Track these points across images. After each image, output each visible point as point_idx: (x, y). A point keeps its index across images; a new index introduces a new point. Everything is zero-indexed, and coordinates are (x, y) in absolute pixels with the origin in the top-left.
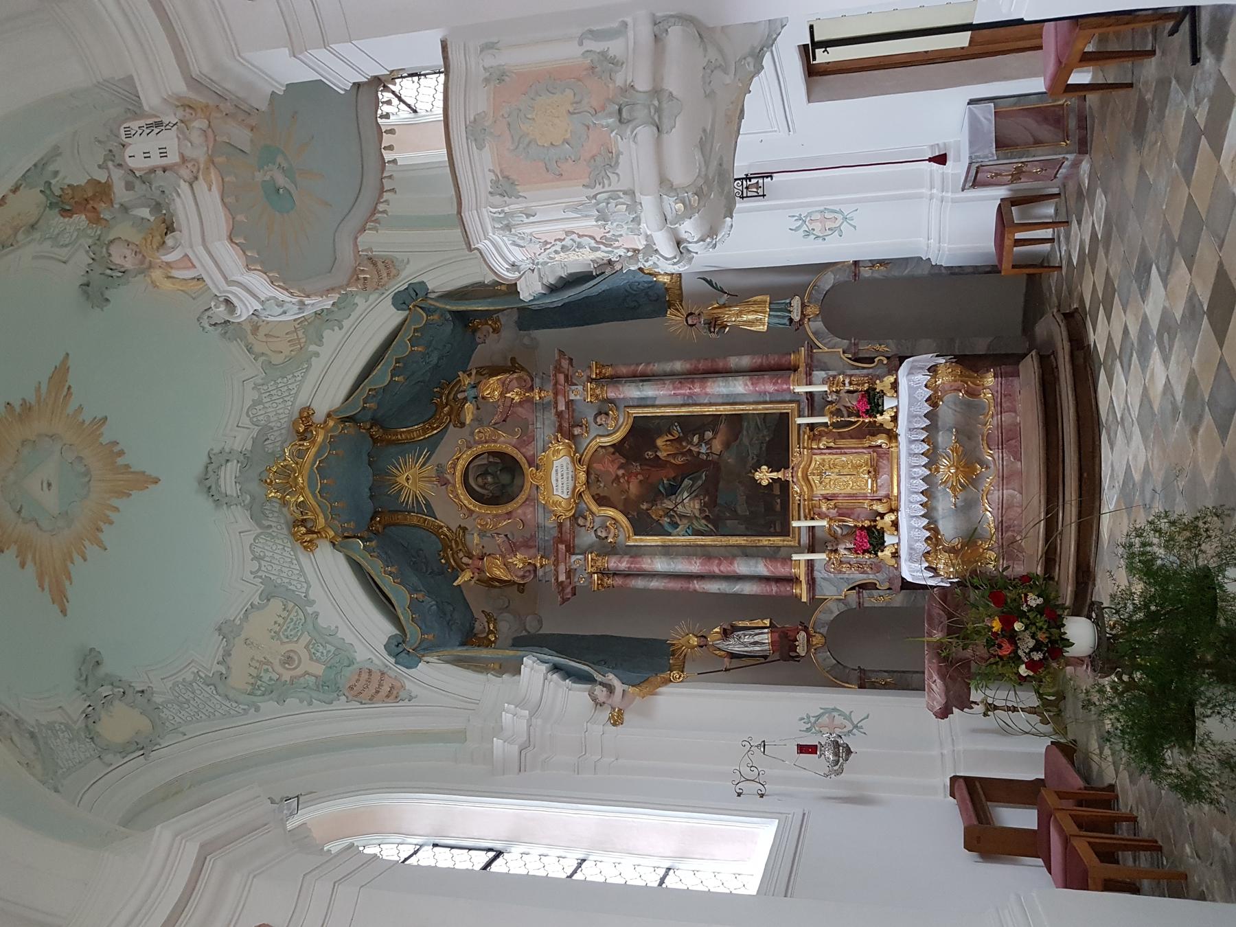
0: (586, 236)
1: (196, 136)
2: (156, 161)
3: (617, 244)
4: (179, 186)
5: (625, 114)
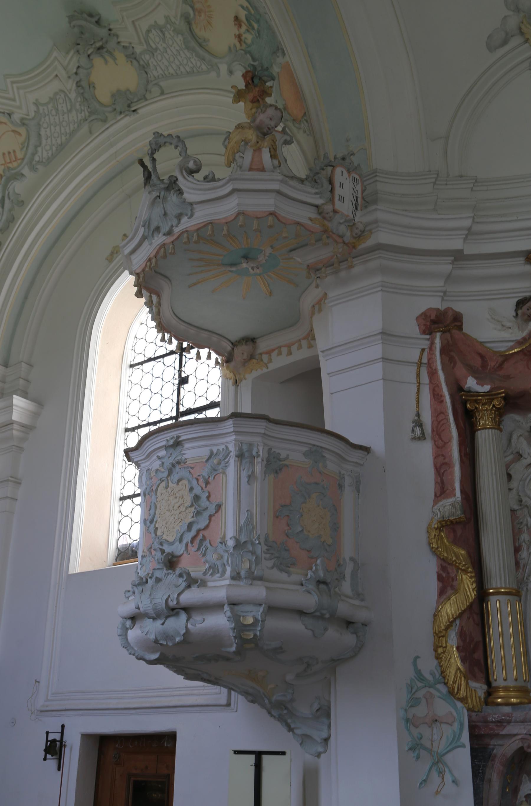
0: (209, 522)
1: (343, 229)
2: (338, 191)
3: (192, 549)
4: (321, 198)
5: (322, 586)
